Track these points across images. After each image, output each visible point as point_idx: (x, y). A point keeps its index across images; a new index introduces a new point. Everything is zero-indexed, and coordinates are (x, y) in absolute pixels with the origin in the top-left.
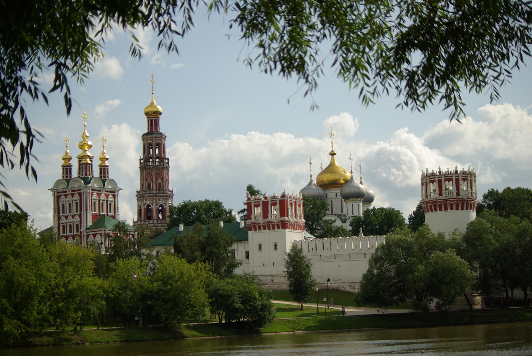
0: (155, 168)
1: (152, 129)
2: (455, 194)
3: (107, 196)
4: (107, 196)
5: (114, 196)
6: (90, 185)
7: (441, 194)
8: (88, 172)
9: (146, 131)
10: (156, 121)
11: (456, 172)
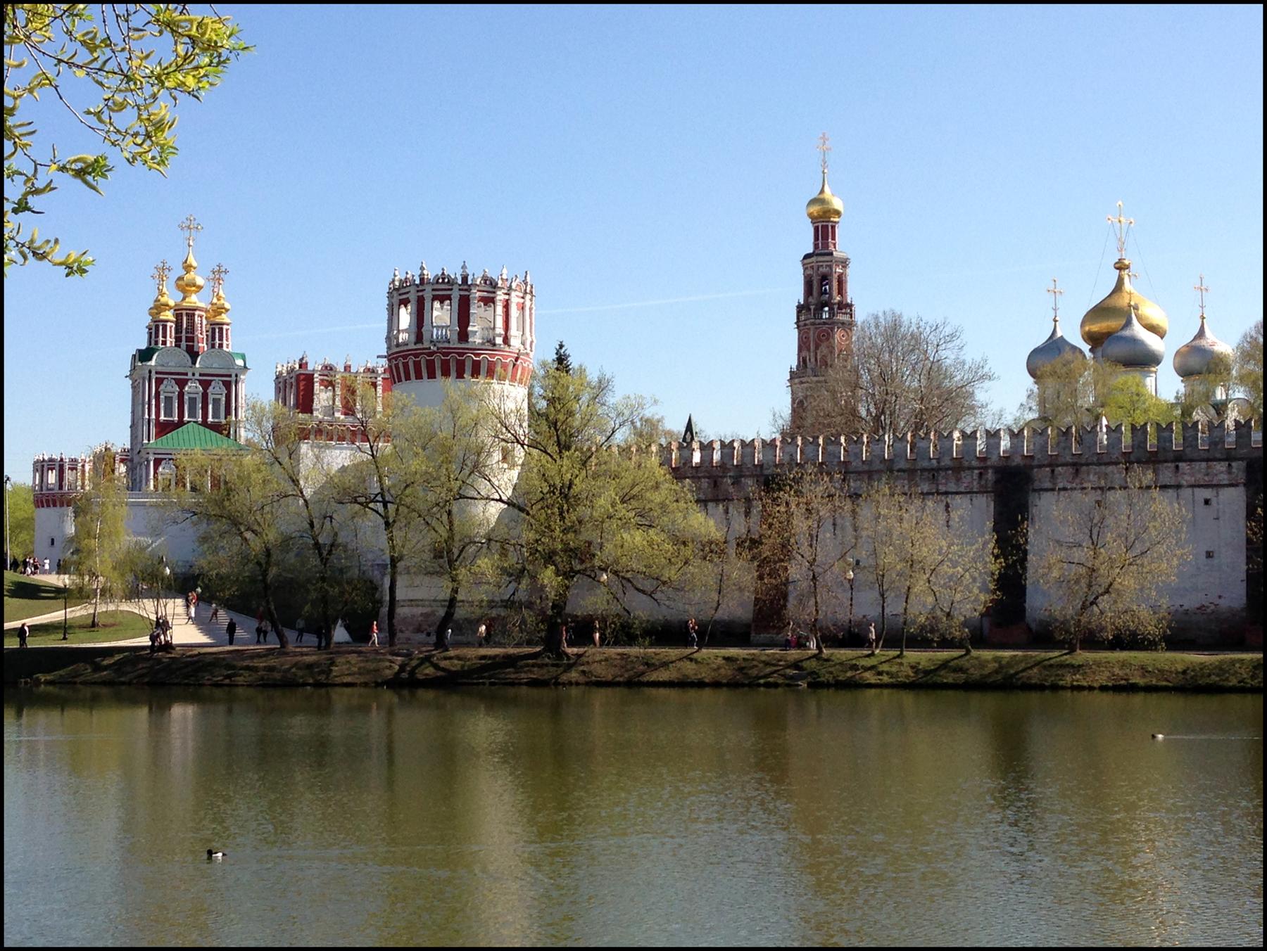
0: (813, 324)
1: (816, 246)
2: (456, 337)
3: (206, 384)
4: (206, 384)
5: (227, 385)
6: (153, 363)
7: (419, 338)
8: (161, 338)
9: (811, 251)
10: (825, 228)
11: (465, 279)
